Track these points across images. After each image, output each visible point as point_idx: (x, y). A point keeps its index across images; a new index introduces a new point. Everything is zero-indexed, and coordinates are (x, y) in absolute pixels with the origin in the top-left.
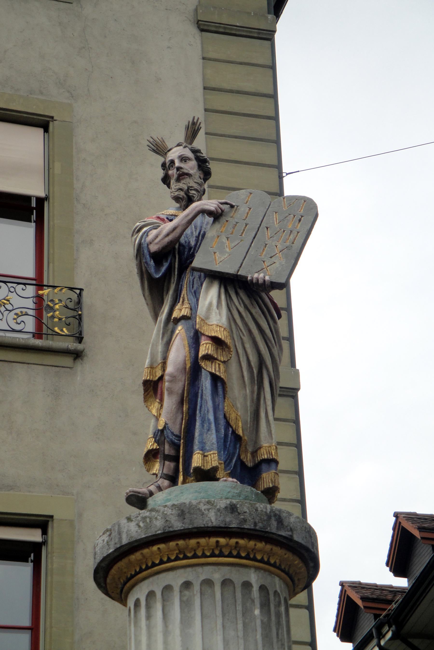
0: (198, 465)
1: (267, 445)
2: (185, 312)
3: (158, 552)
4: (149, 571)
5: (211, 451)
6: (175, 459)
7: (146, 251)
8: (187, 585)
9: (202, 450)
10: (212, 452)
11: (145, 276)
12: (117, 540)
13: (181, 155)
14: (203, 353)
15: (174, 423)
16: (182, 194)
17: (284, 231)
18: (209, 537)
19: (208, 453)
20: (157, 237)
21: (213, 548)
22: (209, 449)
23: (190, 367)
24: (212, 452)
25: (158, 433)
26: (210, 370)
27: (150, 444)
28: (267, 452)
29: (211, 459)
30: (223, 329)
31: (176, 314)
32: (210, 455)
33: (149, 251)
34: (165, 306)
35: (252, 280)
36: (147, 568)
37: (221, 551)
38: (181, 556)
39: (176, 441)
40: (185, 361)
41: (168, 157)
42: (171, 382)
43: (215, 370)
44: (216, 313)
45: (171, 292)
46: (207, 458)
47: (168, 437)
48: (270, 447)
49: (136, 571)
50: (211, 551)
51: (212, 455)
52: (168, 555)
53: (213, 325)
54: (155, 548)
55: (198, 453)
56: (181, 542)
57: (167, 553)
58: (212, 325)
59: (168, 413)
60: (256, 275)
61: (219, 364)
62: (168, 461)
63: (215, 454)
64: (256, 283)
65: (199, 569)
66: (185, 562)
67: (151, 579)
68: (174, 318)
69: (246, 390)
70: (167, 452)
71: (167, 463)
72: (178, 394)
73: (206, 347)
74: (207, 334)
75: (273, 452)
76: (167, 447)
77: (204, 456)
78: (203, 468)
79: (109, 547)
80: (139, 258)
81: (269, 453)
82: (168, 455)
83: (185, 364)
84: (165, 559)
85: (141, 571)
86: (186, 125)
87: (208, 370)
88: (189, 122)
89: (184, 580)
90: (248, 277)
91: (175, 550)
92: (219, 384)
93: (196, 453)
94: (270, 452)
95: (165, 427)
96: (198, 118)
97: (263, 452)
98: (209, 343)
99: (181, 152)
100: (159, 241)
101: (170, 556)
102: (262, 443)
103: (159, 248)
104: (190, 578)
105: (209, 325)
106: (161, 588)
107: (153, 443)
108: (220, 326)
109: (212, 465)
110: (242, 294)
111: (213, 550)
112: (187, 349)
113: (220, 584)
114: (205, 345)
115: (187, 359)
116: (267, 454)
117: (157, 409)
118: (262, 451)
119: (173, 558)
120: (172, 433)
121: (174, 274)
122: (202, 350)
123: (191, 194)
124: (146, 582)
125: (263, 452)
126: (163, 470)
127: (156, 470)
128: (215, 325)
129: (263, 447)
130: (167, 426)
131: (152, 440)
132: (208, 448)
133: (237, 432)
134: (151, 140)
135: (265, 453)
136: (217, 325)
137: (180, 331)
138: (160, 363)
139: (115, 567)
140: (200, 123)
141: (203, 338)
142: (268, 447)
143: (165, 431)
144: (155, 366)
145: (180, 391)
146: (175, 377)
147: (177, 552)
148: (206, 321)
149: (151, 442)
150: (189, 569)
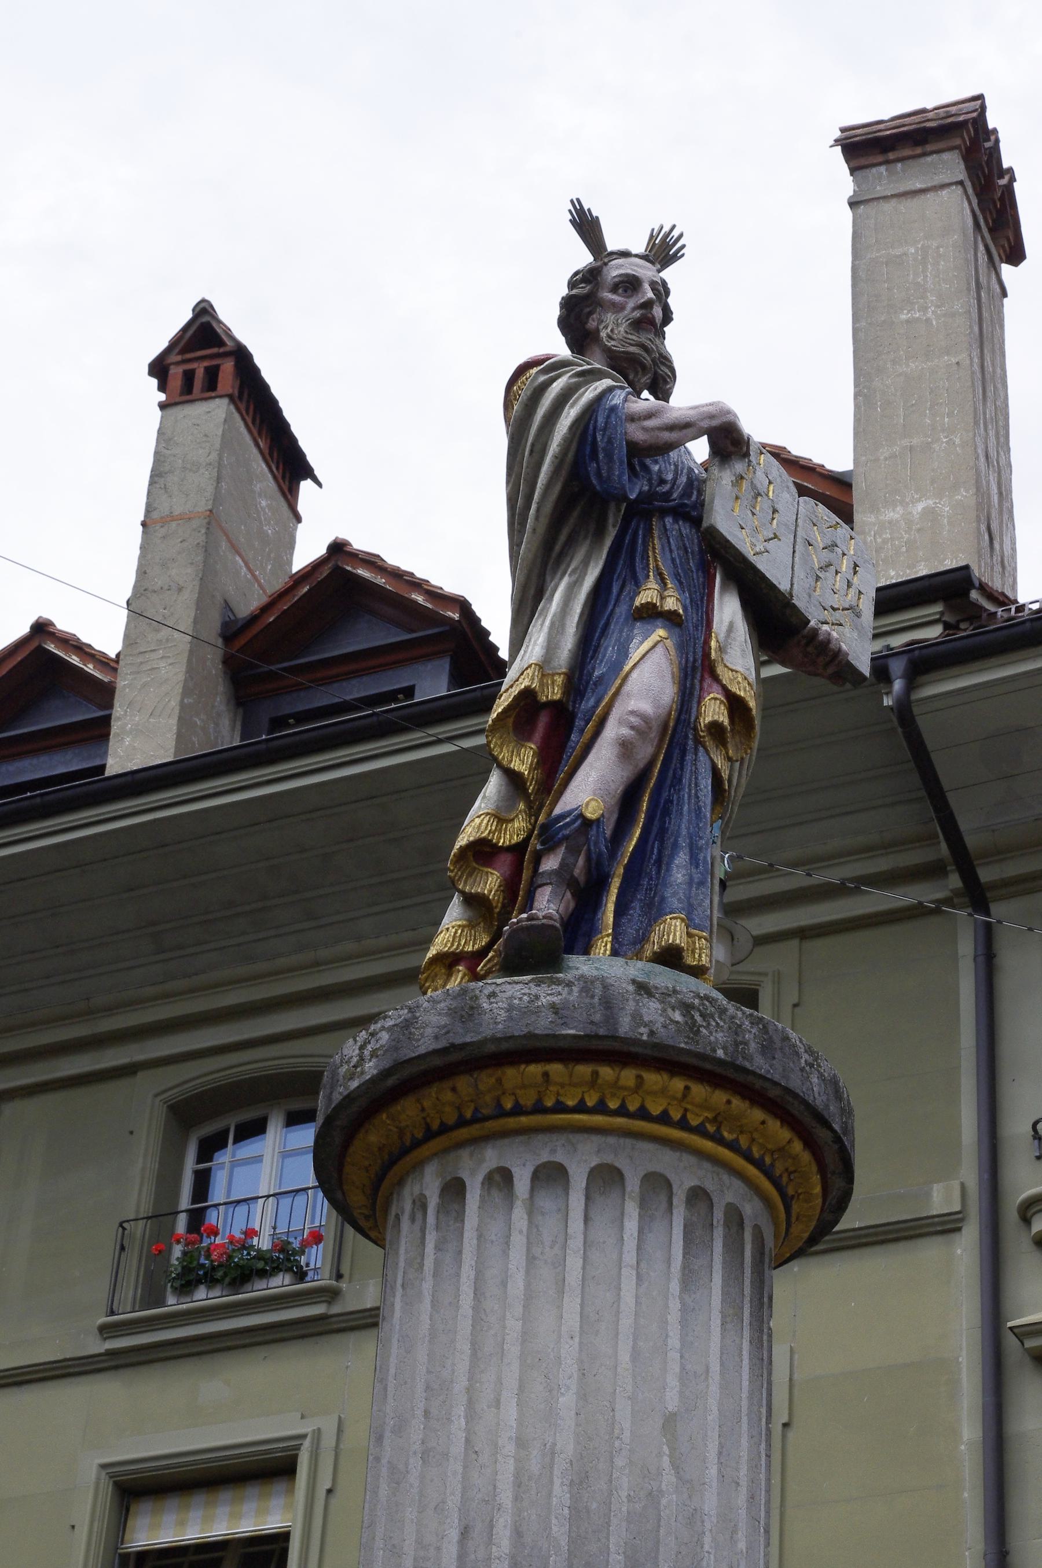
3: (679, 1095)
4: (620, 1121)
5: (702, 931)
8: (698, 1196)
11: (564, 473)
12: (597, 1017)
16: (647, 360)
25: (573, 821)
29: (701, 949)
35: (815, 632)
36: (622, 1111)
40: (671, 707)
42: (640, 734)
45: (608, 542)
47: (596, 843)
49: (582, 1101)
50: (762, 1152)
52: (686, 1110)
53: (737, 672)
55: (683, 920)
57: (689, 1107)
58: (732, 670)
59: (610, 793)
66: (708, 1145)
67: (611, 1140)
70: (577, 872)
76: (581, 861)
79: (560, 1021)
83: (670, 714)
84: (676, 1115)
85: (601, 1108)
86: (653, 230)
90: (809, 621)
93: (680, 918)
95: (598, 820)
96: (681, 236)
100: (653, 429)
101: (689, 1116)
103: (645, 441)
104: (710, 1186)
109: (700, 960)
119: (694, 1122)
124: (597, 1140)
128: (742, 674)
131: (493, 821)
137: (665, 641)
138: (562, 673)
139: (534, 1070)
140: (683, 246)
143: (594, 827)
145: (641, 765)
149: (491, 826)
150: (707, 1165)
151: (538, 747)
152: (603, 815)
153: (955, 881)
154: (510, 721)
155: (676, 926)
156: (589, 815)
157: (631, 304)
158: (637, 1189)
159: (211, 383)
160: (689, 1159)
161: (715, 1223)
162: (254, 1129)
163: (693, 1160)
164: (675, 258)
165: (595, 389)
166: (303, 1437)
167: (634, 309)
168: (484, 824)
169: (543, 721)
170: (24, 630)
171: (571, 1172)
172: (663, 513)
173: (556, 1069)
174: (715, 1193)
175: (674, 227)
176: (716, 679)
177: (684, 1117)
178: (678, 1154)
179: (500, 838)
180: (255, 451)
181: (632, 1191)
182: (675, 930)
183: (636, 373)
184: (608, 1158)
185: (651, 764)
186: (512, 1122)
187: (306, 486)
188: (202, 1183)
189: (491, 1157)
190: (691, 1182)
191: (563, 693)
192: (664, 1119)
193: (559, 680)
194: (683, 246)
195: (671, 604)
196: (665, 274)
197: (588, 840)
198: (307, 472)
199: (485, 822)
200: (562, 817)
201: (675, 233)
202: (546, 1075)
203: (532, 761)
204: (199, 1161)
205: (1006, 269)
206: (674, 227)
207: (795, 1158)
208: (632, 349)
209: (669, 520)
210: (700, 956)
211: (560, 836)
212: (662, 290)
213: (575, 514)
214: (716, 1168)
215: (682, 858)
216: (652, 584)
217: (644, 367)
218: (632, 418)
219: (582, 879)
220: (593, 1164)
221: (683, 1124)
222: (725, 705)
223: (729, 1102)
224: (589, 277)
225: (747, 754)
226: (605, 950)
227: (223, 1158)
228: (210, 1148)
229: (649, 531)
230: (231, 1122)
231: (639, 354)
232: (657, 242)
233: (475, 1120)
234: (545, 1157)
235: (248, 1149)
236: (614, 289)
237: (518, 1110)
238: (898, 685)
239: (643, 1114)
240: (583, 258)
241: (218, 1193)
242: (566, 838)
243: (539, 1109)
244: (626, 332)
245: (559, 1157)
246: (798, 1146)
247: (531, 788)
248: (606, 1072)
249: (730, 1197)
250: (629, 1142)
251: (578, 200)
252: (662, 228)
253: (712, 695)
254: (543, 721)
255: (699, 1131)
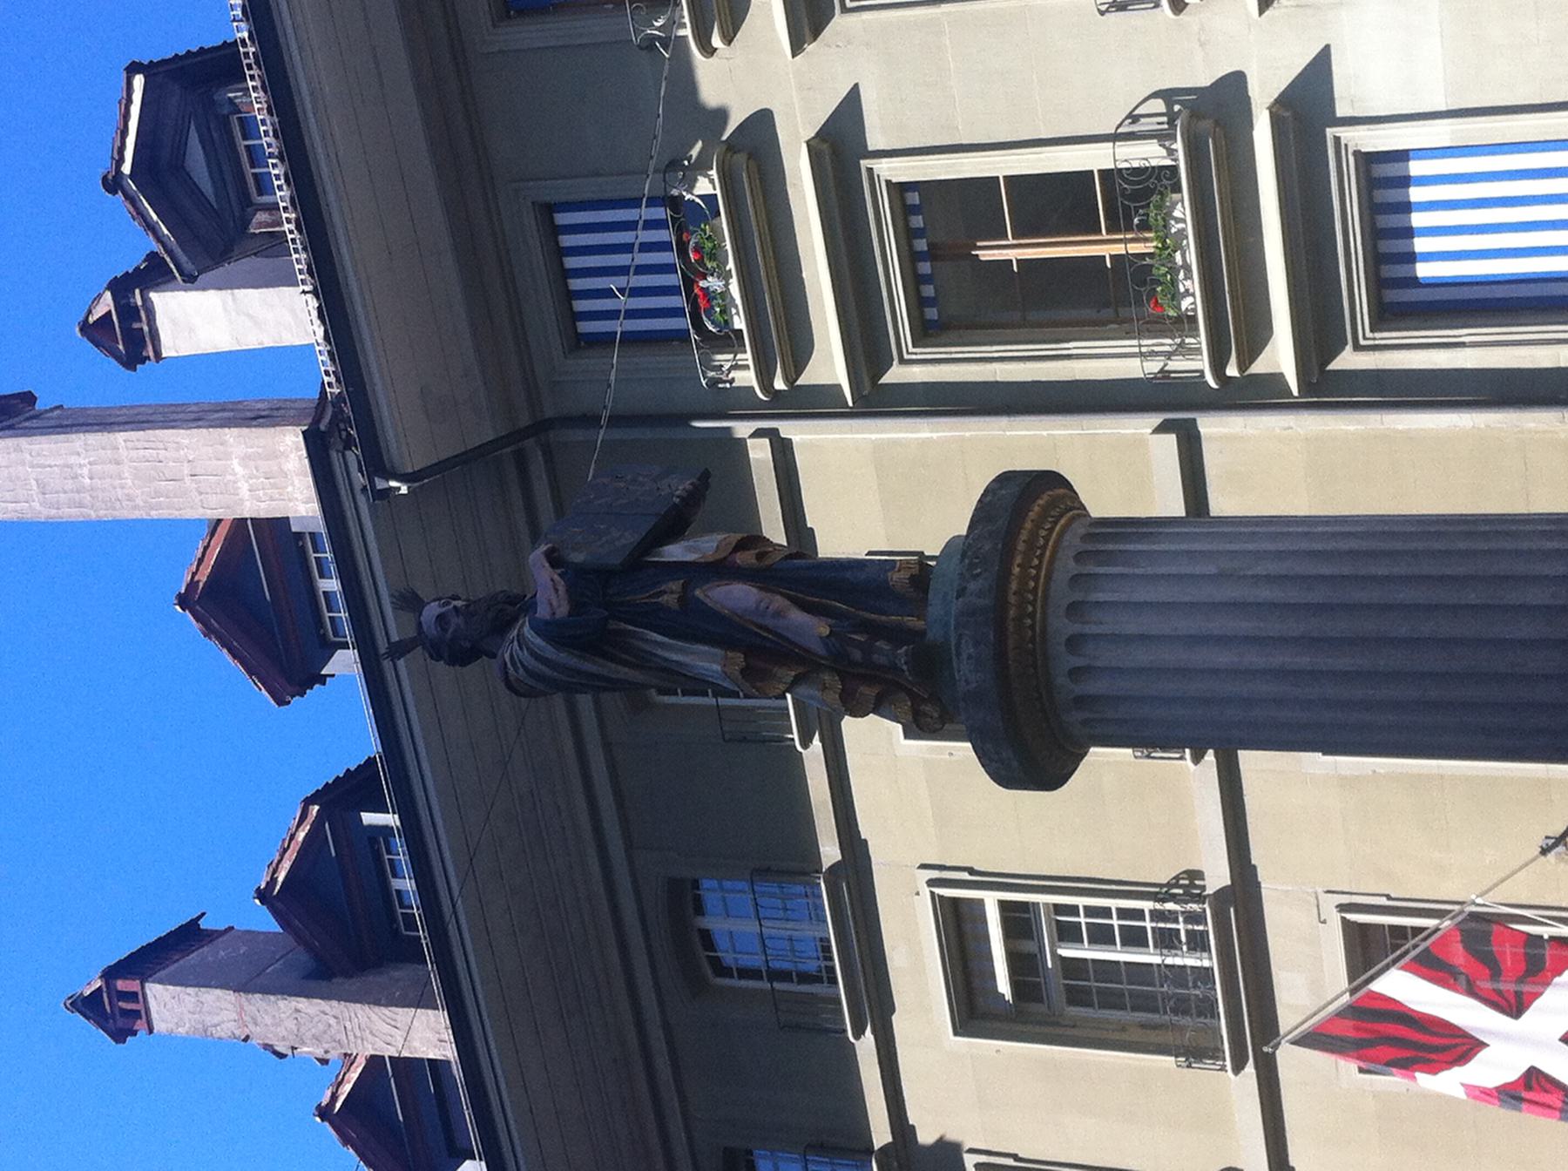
2: (676, 586)
6: (875, 630)
104: (1072, 553)
153: (530, 443)
159: (132, 996)
162: (707, 938)
166: (932, 893)
171: (1071, 633)
176: (725, 558)
180: (181, 962)
187: (203, 924)
188: (745, 973)
189: (1061, 680)
198: (194, 923)
201: (397, 594)
204: (732, 976)
205: (39, 406)
209: (611, 591)
227: (728, 958)
228: (721, 970)
230: (703, 954)
234: (1063, 648)
235: (722, 943)
236: (445, 630)
238: (393, 484)
241: (756, 961)
249: (1077, 541)
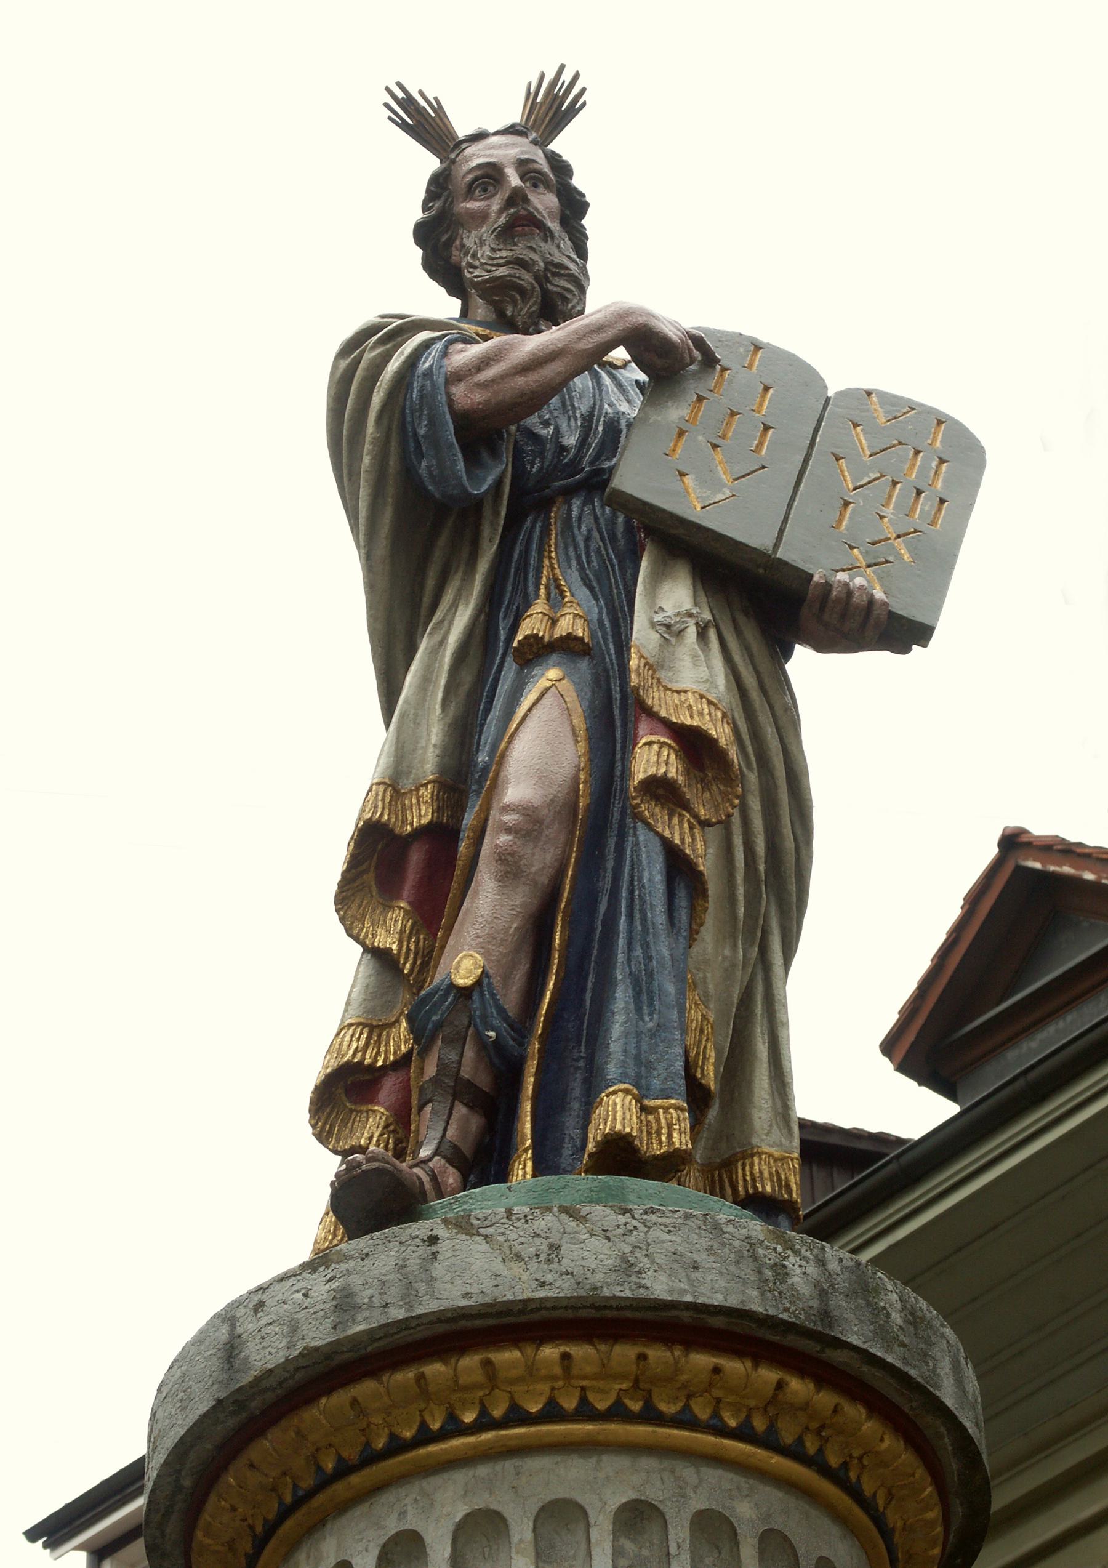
0: (628, 1130)
1: (776, 1152)
3: (558, 1370)
5: (668, 1098)
7: (442, 398)
9: (636, 1085)
10: (673, 1101)
11: (391, 490)
13: (528, 161)
14: (652, 771)
15: (506, 978)
16: (526, 278)
17: (895, 483)
18: (757, 1362)
19: (659, 1102)
20: (484, 362)
21: (752, 1403)
22: (662, 1090)
23: (588, 808)
24: (673, 1101)
26: (667, 833)
27: (354, 1045)
28: (771, 1174)
29: (670, 1126)
30: (719, 714)
31: (532, 625)
32: (666, 1109)
33: (451, 403)
34: (454, 606)
36: (485, 1423)
37: (772, 1427)
38: (635, 1406)
39: (511, 1042)
40: (576, 780)
41: (468, 159)
42: (524, 836)
43: (682, 840)
44: (695, 657)
45: (483, 566)
46: (651, 1118)
48: (783, 1159)
49: (423, 1425)
50: (743, 1416)
51: (672, 1111)
52: (583, 1389)
53: (686, 692)
54: (550, 1352)
55: (626, 1092)
56: (658, 1355)
57: (584, 1383)
58: (678, 692)
59: (495, 938)
60: (842, 576)
61: (691, 828)
62: (466, 1105)
63: (682, 1110)
64: (838, 600)
65: (688, 1472)
66: (642, 1431)
67: (483, 1470)
68: (526, 637)
69: (734, 947)
70: (466, 1073)
71: (460, 1110)
72: (536, 883)
73: (659, 754)
74: (663, 714)
75: (792, 1179)
76: (469, 1053)
77: (643, 1109)
78: (637, 1142)
80: (385, 421)
81: (779, 1179)
82: (469, 1084)
84: (569, 1403)
85: (454, 1428)
86: (530, 84)
87: (659, 830)
88: (542, 77)
89: (632, 1495)
90: (812, 576)
91: (622, 1377)
92: (682, 895)
93: (620, 1090)
94: (783, 1177)
95: (478, 983)
96: (576, 77)
97: (761, 1172)
98: (669, 746)
99: (526, 153)
100: (494, 381)
101: (591, 1397)
102: (755, 1141)
103: (487, 402)
104: (655, 1493)
105: (667, 689)
106: (534, 1506)
107: (362, 1042)
108: (710, 702)
110: (751, 634)
111: (749, 1417)
112: (582, 747)
113: (755, 1541)
114: (656, 747)
115: (582, 777)
116: (772, 1181)
117: (402, 932)
118: (758, 1165)
119: (602, 1404)
120: (501, 1011)
121: (497, 514)
122: (648, 761)
123: (550, 287)
124: (460, 1477)
125: (761, 1172)
126: (445, 1130)
127: (371, 1138)
129: (760, 1154)
130: (485, 981)
131: (361, 1033)
132: (656, 1083)
133: (699, 1075)
134: (400, 94)
135: (766, 1174)
136: (702, 697)
137: (557, 684)
138: (429, 782)
139: (339, 1399)
140: (583, 90)
141: (643, 726)
142: (776, 1160)
143: (476, 996)
144: (407, 785)
145: (544, 880)
146: (538, 822)
147: (624, 1386)
148: (661, 674)
149: (358, 1040)
150: (648, 1463)
151: (410, 903)
152: (484, 973)
154: (370, 878)
155: (615, 1104)
156: (461, 982)
157: (496, 204)
158: (529, 1535)
160: (612, 1464)
161: (673, 1549)
163: (622, 1461)
164: (573, 111)
165: (402, 353)
167: (500, 212)
168: (346, 1043)
169: (416, 858)
170: (992, 851)
171: (428, 1539)
172: (568, 493)
173: (365, 1389)
174: (669, 1503)
175: (562, 68)
177: (584, 1401)
178: (593, 1460)
179: (378, 1053)
181: (521, 1541)
182: (615, 1112)
183: (515, 305)
184: (480, 1502)
185: (561, 872)
186: (340, 1489)
190: (617, 1499)
191: (438, 810)
192: (552, 1413)
193: (426, 793)
194: (583, 90)
195: (567, 625)
196: (562, 145)
197: (471, 1017)
199: (348, 1038)
200: (431, 995)
201: (567, 77)
202: (354, 1402)
203: (404, 927)
206: (562, 68)
207: (806, 1406)
208: (502, 271)
210: (670, 1136)
211: (430, 1026)
212: (562, 168)
213: (442, 541)
214: (666, 1463)
215: (622, 998)
216: (540, 606)
217: (522, 291)
218: (457, 377)
219: (483, 1081)
220: (459, 1517)
221: (586, 1412)
222: (669, 746)
223: (642, 1357)
224: (439, 186)
225: (734, 807)
226: (525, 1174)
229: (546, 532)
231: (510, 275)
232: (539, 100)
233: (299, 1502)
234: (393, 1526)
237: (344, 1470)
239: (517, 1416)
240: (431, 163)
242: (439, 1025)
243: (370, 1458)
244: (493, 250)
245: (413, 1522)
246: (798, 1387)
247: (408, 966)
248: (435, 1369)
249: (699, 1502)
250: (509, 1465)
251: (400, 85)
252: (542, 77)
253: (643, 741)
254: (416, 858)
255: (617, 1413)
